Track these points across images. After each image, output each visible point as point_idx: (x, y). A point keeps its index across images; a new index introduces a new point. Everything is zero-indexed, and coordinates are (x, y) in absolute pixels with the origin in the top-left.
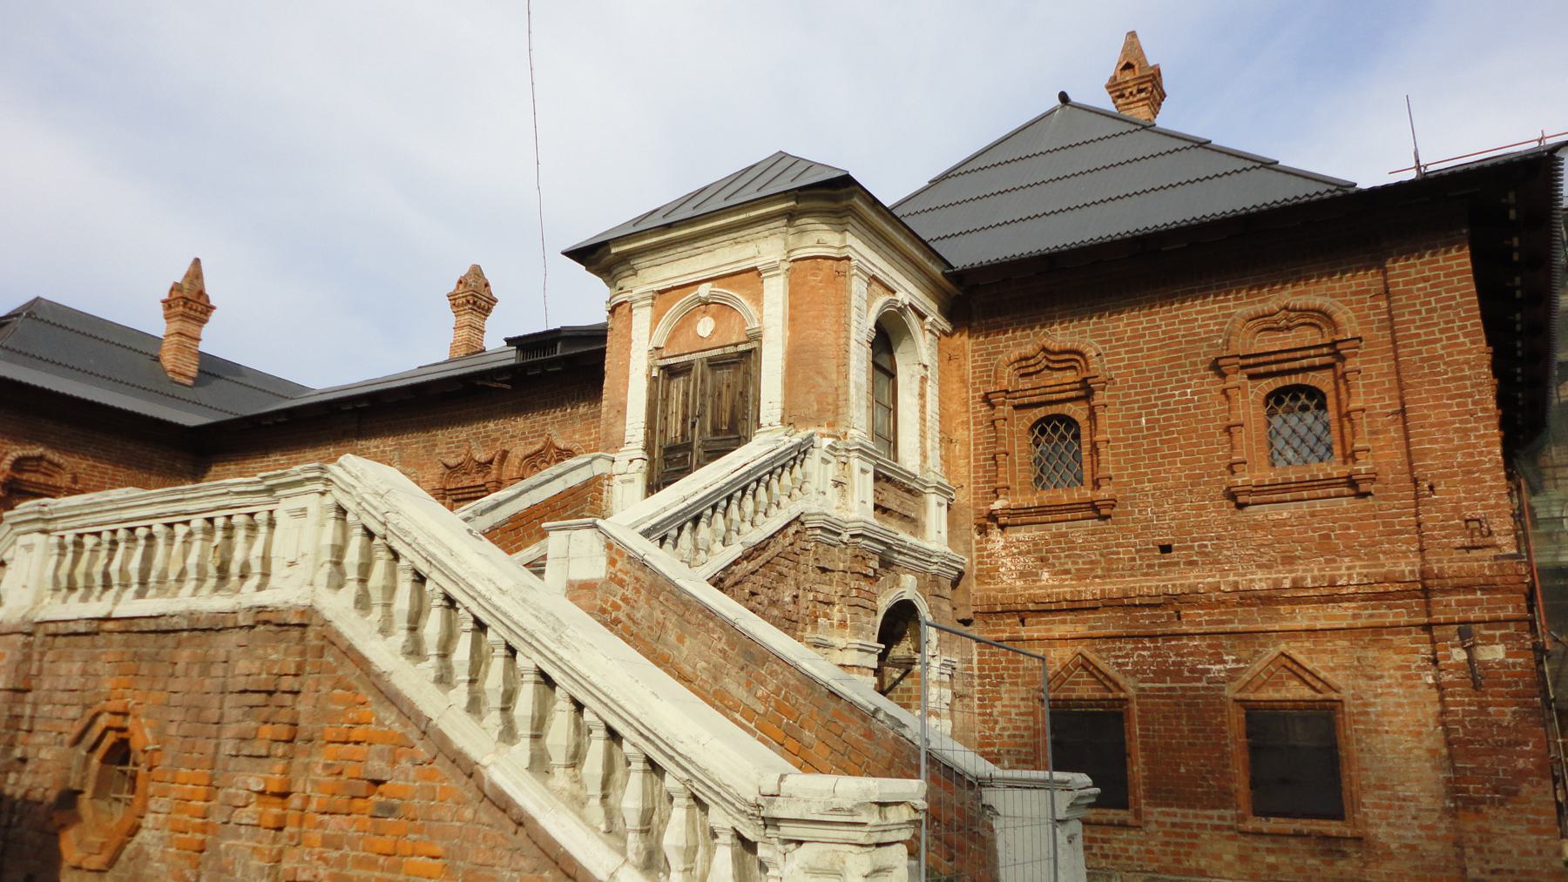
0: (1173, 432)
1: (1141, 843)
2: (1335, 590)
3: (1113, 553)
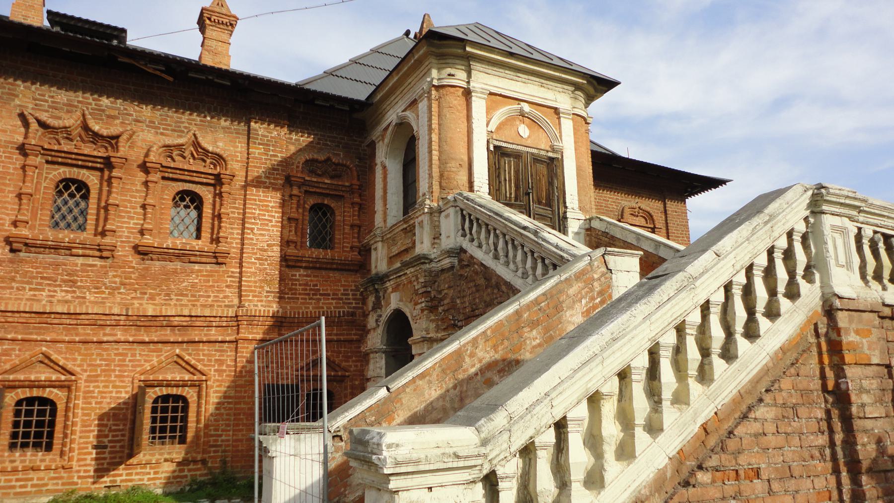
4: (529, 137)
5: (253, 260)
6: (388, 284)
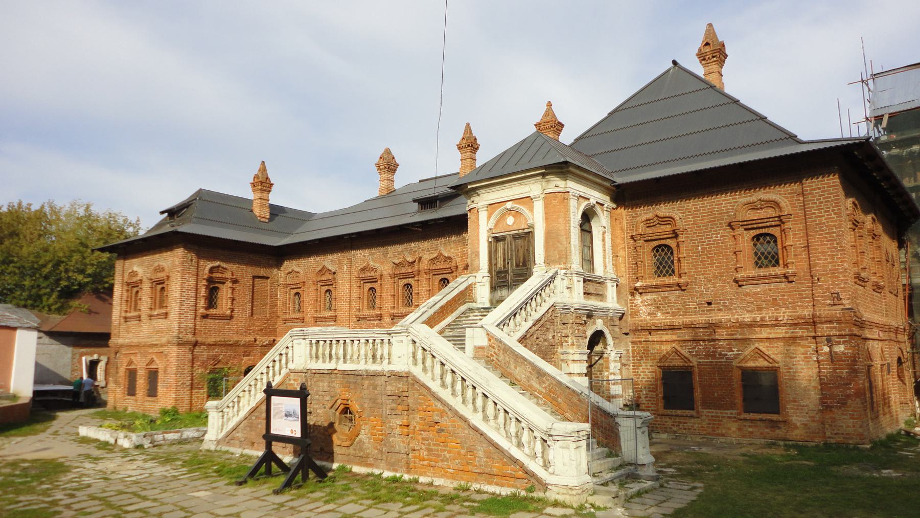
0: (712, 254)
1: (699, 423)
2: (778, 322)
3: (687, 305)
4: (514, 223)
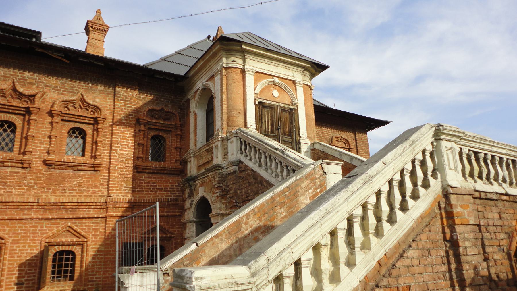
4: (278, 97)
5: (117, 169)
6: (197, 182)
